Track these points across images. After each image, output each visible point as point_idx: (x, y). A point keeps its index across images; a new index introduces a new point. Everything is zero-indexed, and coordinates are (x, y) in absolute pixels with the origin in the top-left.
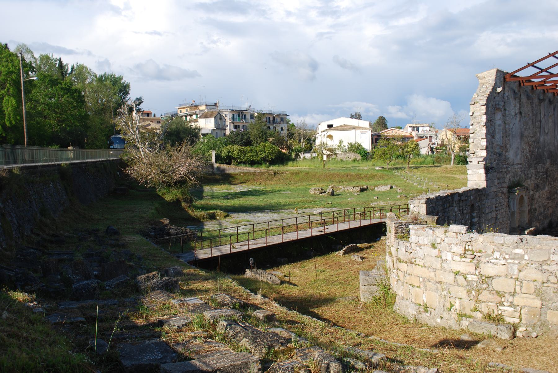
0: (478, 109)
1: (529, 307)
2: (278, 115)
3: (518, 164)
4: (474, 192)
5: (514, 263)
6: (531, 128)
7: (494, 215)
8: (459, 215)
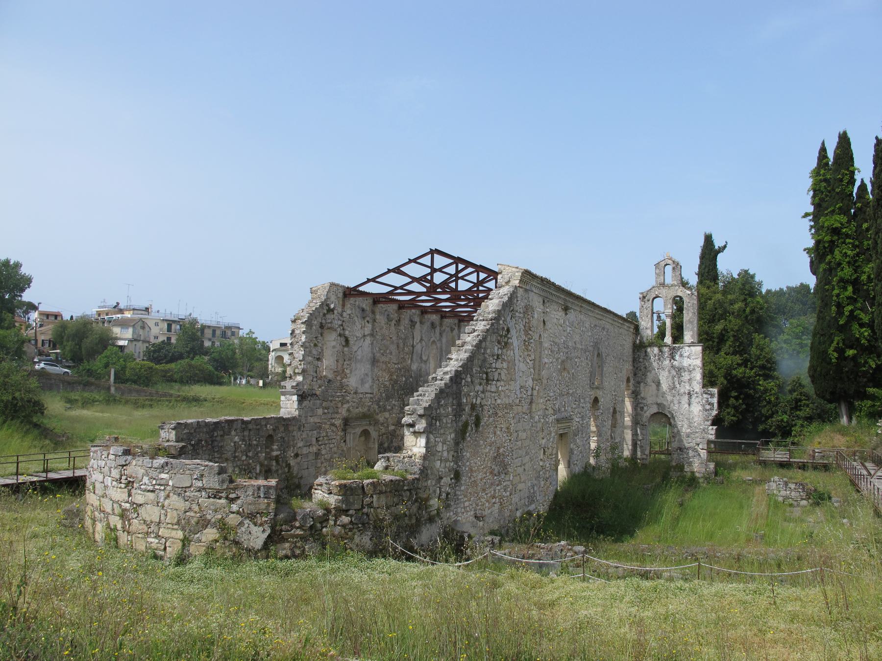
0: (299, 326)
1: (172, 538)
2: (229, 328)
3: (366, 393)
4: (273, 421)
5: (160, 490)
6: (394, 354)
7: (314, 449)
8: (243, 446)
